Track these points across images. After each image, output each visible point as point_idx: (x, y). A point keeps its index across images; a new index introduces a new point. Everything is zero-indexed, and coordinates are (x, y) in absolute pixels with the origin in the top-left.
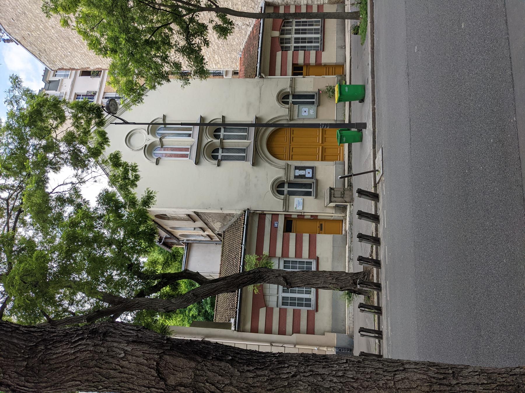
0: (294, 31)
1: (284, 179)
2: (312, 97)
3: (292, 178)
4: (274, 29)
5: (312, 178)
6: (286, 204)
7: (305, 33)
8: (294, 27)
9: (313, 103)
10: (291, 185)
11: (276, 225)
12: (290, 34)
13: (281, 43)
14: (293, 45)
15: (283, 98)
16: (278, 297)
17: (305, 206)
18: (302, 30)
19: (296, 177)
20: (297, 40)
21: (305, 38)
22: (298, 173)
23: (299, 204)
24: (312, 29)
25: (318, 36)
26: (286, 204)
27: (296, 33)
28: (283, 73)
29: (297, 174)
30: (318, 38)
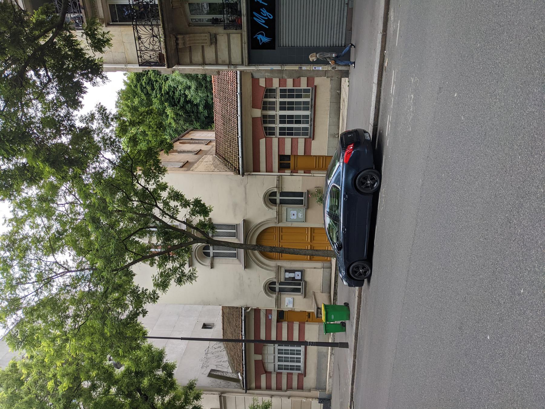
0: (278, 106)
1: (275, 280)
2: (301, 194)
3: (283, 280)
4: (254, 106)
5: (301, 280)
6: (278, 302)
7: (291, 109)
8: (279, 100)
9: (300, 202)
10: (281, 283)
11: (270, 317)
12: (274, 109)
13: (265, 122)
14: (278, 125)
15: (270, 199)
16: (274, 356)
17: (295, 304)
18: (289, 103)
19: (286, 279)
20: (283, 119)
21: (291, 117)
22: (288, 275)
23: (289, 302)
24: (299, 103)
25: (307, 113)
26: (278, 302)
27: (281, 109)
28: (269, 169)
29: (287, 277)
30: (307, 117)
